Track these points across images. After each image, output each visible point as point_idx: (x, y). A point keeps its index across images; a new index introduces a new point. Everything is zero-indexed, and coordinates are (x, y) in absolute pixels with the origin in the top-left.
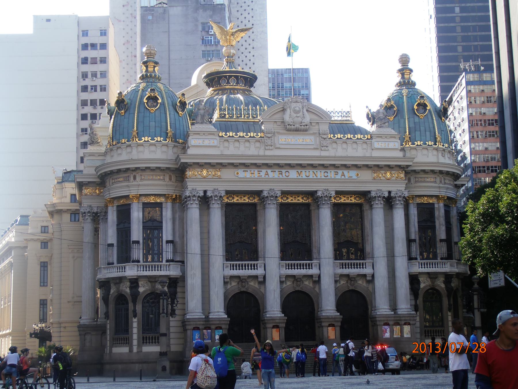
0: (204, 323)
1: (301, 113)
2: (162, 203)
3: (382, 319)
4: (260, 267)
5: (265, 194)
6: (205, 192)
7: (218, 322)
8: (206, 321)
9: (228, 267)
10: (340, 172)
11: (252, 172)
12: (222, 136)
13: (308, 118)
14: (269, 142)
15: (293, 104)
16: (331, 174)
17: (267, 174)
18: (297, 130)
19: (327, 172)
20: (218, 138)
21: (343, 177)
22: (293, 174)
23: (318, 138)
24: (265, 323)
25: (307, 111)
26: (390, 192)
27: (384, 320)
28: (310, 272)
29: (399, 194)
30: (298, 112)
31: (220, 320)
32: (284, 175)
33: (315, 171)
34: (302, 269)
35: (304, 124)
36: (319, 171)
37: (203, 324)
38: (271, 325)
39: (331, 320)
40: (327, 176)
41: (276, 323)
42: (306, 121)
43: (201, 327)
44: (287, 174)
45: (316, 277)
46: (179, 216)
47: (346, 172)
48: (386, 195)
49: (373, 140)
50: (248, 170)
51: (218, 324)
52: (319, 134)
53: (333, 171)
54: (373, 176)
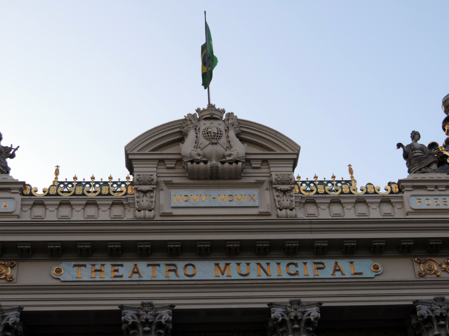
1: (223, 140)
5: (129, 316)
10: (329, 264)
11: (98, 267)
12: (31, 194)
13: (239, 149)
14: (145, 201)
15: (202, 122)
16: (306, 269)
17: (136, 272)
19: (296, 265)
20: (18, 197)
21: (338, 275)
22: (205, 270)
23: (267, 193)
25: (238, 136)
30: (218, 136)
32: (181, 272)
33: (263, 263)
35: (228, 158)
36: (273, 264)
40: (297, 273)
42: (234, 153)
44: (190, 270)
47: (344, 264)
49: (406, 195)
50: (88, 264)
52: (271, 183)
53: (310, 263)
54: (417, 271)
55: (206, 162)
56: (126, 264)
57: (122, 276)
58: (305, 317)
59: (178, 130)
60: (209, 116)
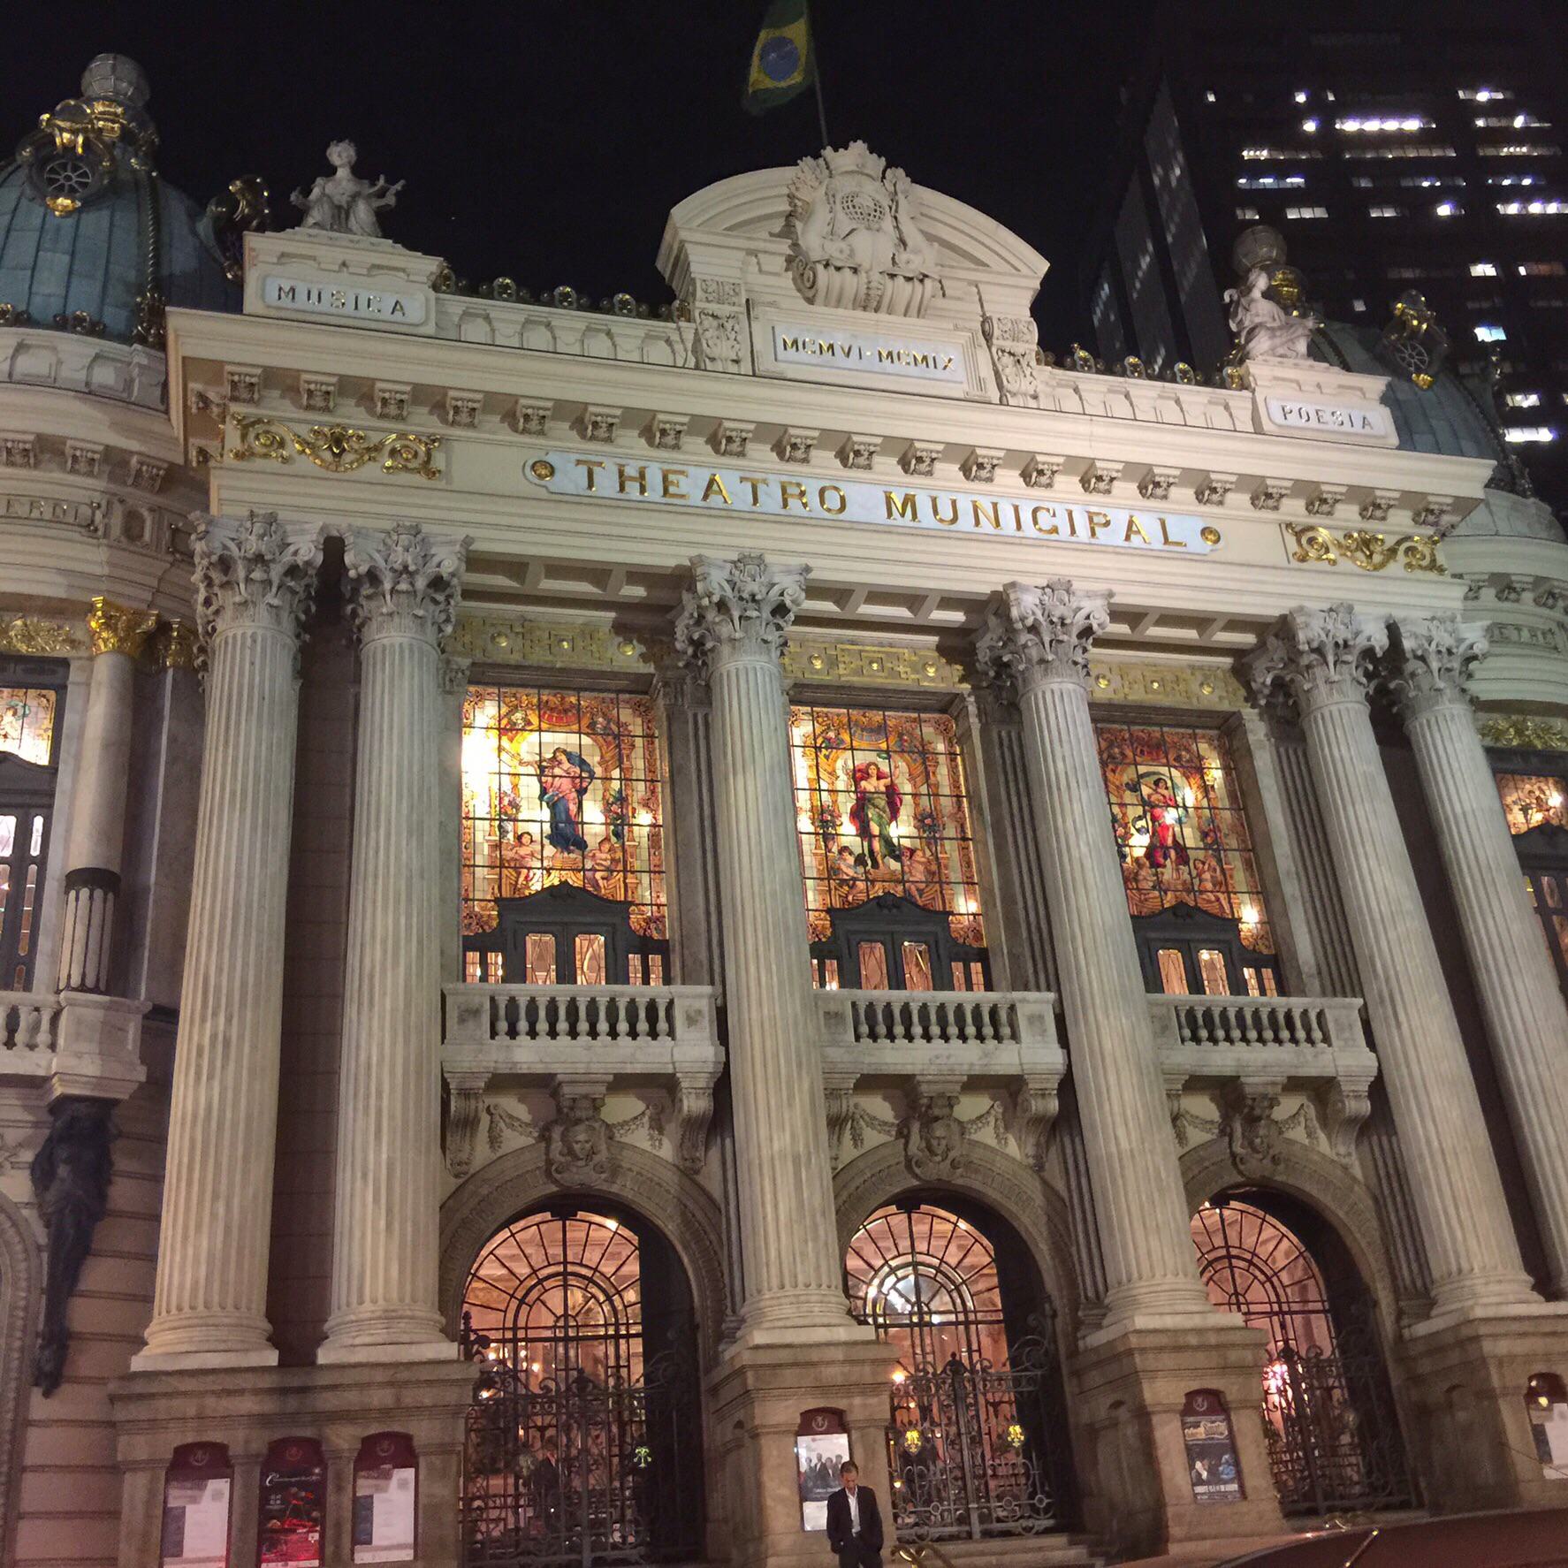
0: (268, 1406)
2: (64, 663)
3: (1520, 1347)
4: (691, 1020)
5: (715, 582)
6: (333, 546)
7: (380, 1398)
8: (283, 1391)
9: (476, 1013)
18: (869, 302)
24: (746, 1397)
26: (1393, 630)
27: (1529, 1358)
28: (1004, 1058)
29: (1444, 639)
31: (399, 1375)
34: (956, 1043)
37: (263, 1420)
38: (784, 1411)
39: (1201, 1359)
40: (1055, 530)
41: (823, 1389)
43: (238, 1440)
45: (1043, 1094)
46: (172, 740)
48: (1380, 641)
51: (385, 1413)
55: (855, 271)
56: (691, 470)
57: (683, 496)
58: (1079, 621)
59: (786, 191)
60: (854, 168)
